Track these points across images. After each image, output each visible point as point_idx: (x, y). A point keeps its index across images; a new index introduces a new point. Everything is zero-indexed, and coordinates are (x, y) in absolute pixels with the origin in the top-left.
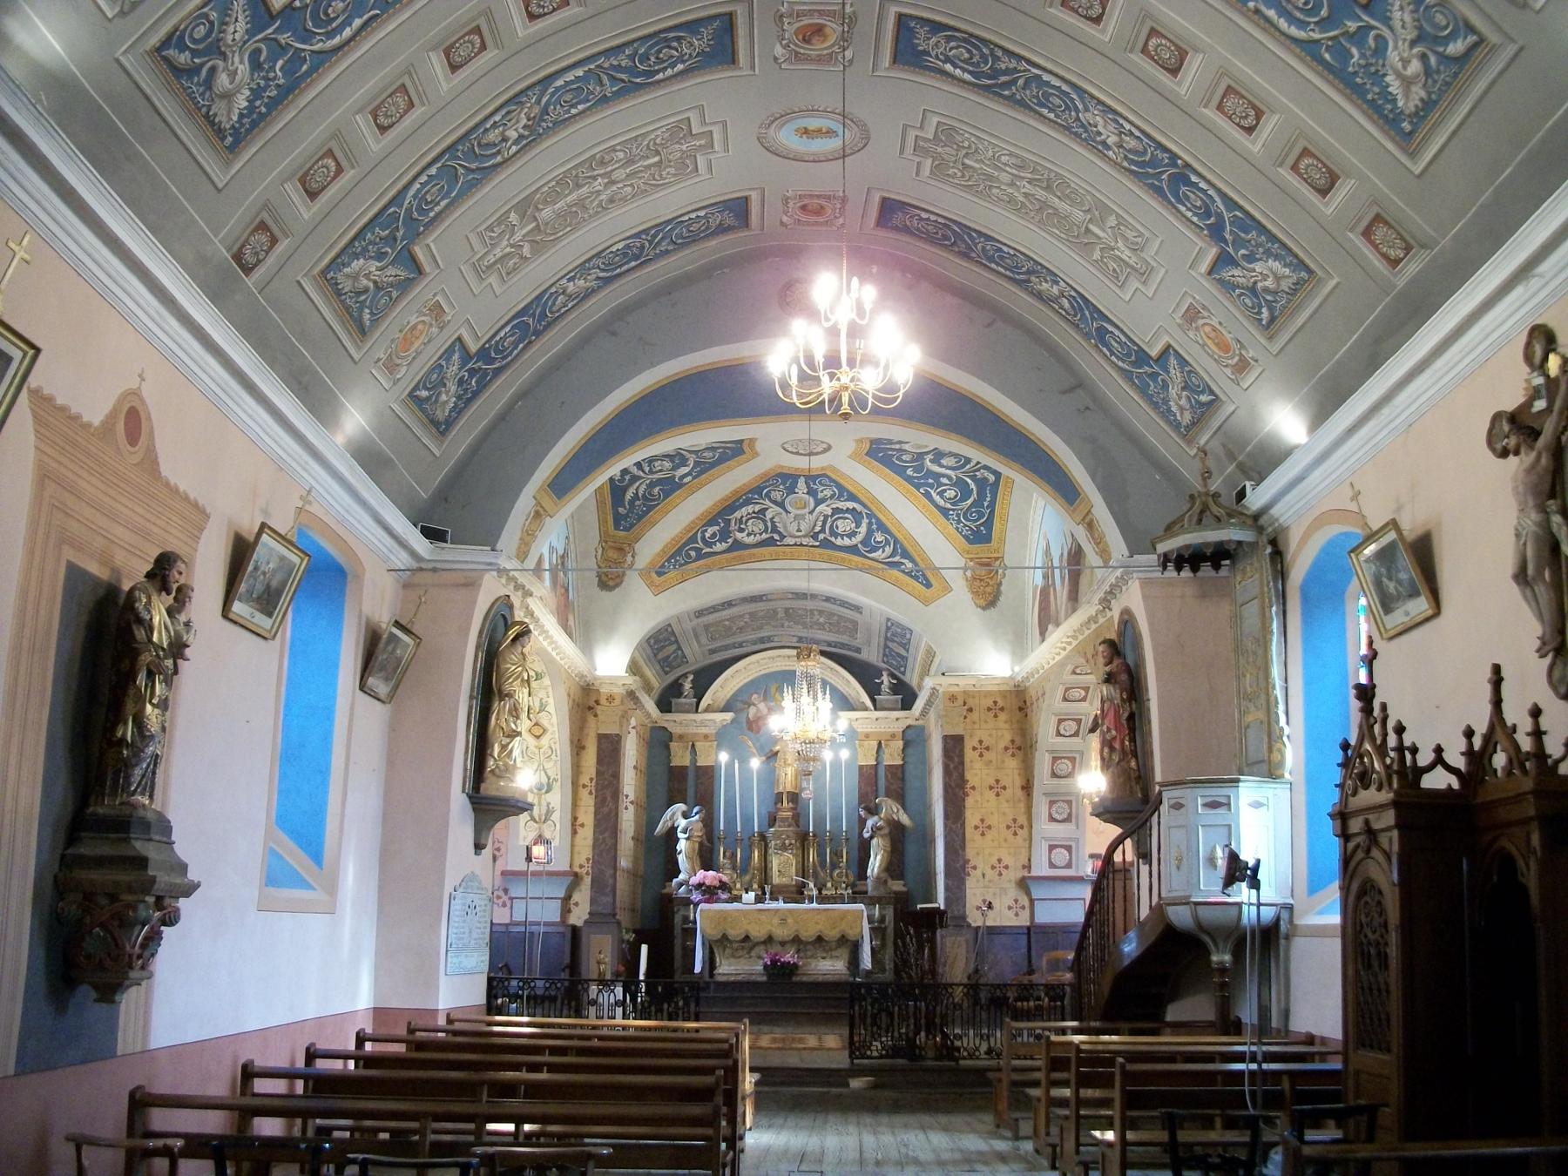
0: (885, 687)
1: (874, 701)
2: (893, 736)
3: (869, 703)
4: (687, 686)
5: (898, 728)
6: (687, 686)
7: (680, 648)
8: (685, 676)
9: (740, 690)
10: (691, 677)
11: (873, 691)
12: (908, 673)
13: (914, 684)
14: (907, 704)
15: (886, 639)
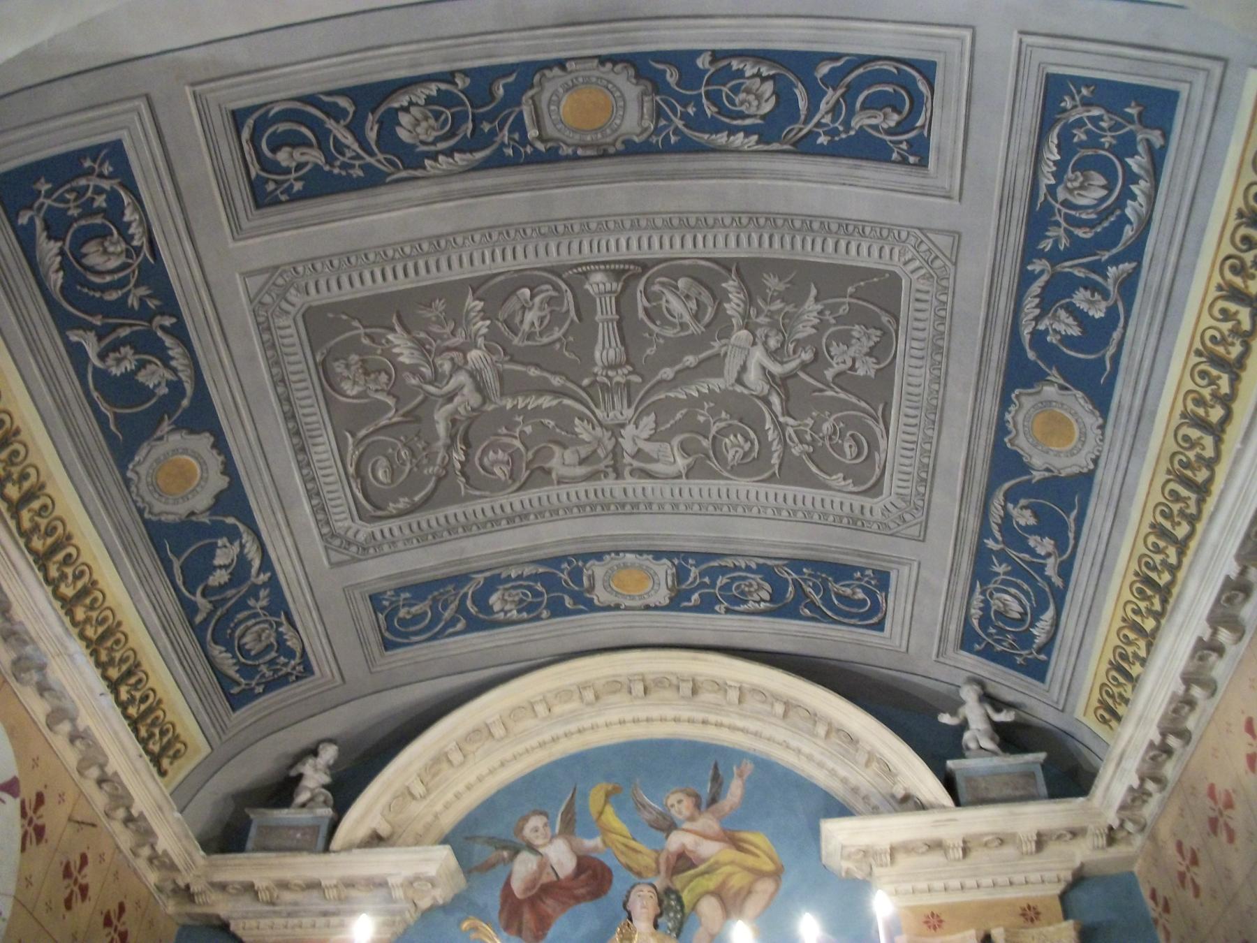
0: (978, 733)
1: (949, 783)
2: (1030, 914)
3: (928, 785)
4: (314, 776)
5: (1044, 878)
6: (314, 776)
7: (233, 500)
8: (314, 752)
9: (489, 807)
10: (329, 754)
11: (938, 748)
12: (1059, 665)
13: (1082, 716)
14: (1069, 775)
15: (1019, 373)
